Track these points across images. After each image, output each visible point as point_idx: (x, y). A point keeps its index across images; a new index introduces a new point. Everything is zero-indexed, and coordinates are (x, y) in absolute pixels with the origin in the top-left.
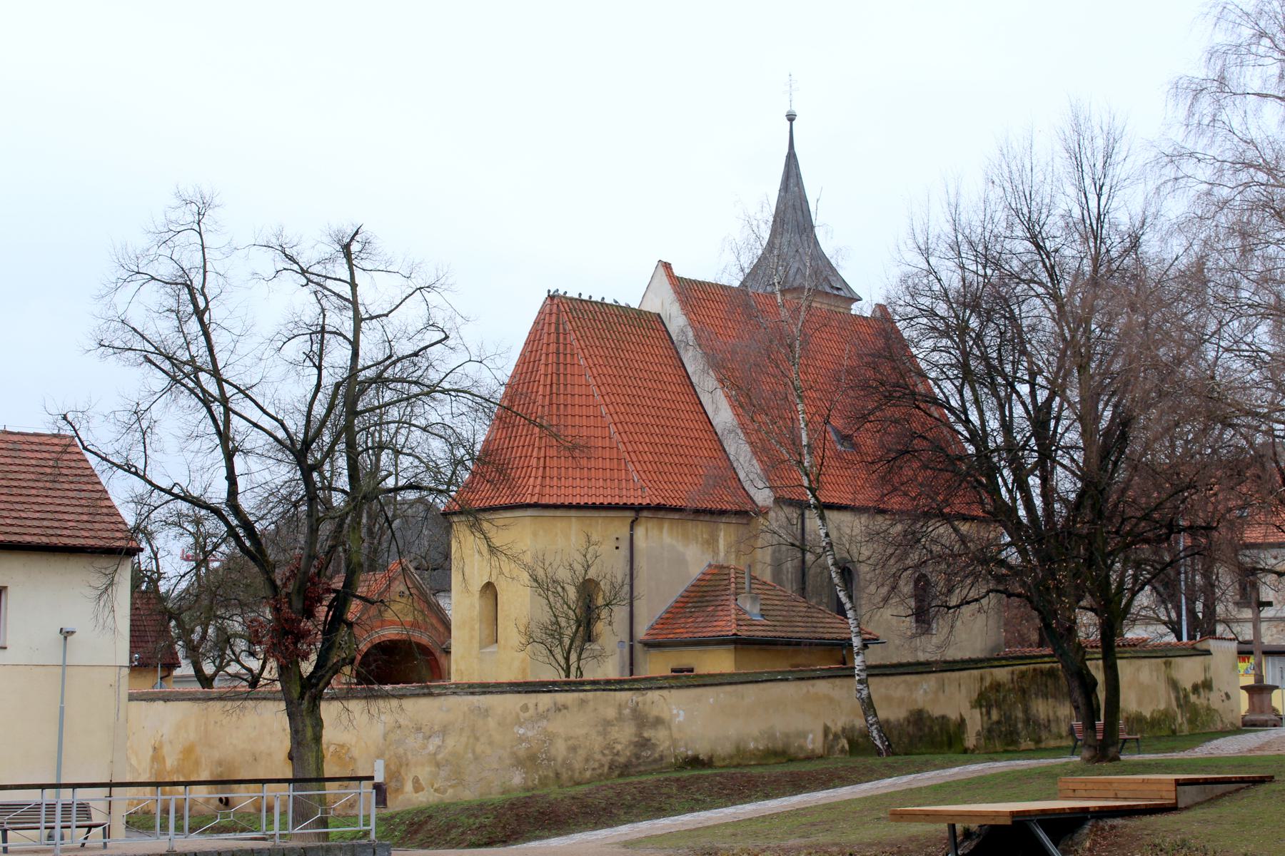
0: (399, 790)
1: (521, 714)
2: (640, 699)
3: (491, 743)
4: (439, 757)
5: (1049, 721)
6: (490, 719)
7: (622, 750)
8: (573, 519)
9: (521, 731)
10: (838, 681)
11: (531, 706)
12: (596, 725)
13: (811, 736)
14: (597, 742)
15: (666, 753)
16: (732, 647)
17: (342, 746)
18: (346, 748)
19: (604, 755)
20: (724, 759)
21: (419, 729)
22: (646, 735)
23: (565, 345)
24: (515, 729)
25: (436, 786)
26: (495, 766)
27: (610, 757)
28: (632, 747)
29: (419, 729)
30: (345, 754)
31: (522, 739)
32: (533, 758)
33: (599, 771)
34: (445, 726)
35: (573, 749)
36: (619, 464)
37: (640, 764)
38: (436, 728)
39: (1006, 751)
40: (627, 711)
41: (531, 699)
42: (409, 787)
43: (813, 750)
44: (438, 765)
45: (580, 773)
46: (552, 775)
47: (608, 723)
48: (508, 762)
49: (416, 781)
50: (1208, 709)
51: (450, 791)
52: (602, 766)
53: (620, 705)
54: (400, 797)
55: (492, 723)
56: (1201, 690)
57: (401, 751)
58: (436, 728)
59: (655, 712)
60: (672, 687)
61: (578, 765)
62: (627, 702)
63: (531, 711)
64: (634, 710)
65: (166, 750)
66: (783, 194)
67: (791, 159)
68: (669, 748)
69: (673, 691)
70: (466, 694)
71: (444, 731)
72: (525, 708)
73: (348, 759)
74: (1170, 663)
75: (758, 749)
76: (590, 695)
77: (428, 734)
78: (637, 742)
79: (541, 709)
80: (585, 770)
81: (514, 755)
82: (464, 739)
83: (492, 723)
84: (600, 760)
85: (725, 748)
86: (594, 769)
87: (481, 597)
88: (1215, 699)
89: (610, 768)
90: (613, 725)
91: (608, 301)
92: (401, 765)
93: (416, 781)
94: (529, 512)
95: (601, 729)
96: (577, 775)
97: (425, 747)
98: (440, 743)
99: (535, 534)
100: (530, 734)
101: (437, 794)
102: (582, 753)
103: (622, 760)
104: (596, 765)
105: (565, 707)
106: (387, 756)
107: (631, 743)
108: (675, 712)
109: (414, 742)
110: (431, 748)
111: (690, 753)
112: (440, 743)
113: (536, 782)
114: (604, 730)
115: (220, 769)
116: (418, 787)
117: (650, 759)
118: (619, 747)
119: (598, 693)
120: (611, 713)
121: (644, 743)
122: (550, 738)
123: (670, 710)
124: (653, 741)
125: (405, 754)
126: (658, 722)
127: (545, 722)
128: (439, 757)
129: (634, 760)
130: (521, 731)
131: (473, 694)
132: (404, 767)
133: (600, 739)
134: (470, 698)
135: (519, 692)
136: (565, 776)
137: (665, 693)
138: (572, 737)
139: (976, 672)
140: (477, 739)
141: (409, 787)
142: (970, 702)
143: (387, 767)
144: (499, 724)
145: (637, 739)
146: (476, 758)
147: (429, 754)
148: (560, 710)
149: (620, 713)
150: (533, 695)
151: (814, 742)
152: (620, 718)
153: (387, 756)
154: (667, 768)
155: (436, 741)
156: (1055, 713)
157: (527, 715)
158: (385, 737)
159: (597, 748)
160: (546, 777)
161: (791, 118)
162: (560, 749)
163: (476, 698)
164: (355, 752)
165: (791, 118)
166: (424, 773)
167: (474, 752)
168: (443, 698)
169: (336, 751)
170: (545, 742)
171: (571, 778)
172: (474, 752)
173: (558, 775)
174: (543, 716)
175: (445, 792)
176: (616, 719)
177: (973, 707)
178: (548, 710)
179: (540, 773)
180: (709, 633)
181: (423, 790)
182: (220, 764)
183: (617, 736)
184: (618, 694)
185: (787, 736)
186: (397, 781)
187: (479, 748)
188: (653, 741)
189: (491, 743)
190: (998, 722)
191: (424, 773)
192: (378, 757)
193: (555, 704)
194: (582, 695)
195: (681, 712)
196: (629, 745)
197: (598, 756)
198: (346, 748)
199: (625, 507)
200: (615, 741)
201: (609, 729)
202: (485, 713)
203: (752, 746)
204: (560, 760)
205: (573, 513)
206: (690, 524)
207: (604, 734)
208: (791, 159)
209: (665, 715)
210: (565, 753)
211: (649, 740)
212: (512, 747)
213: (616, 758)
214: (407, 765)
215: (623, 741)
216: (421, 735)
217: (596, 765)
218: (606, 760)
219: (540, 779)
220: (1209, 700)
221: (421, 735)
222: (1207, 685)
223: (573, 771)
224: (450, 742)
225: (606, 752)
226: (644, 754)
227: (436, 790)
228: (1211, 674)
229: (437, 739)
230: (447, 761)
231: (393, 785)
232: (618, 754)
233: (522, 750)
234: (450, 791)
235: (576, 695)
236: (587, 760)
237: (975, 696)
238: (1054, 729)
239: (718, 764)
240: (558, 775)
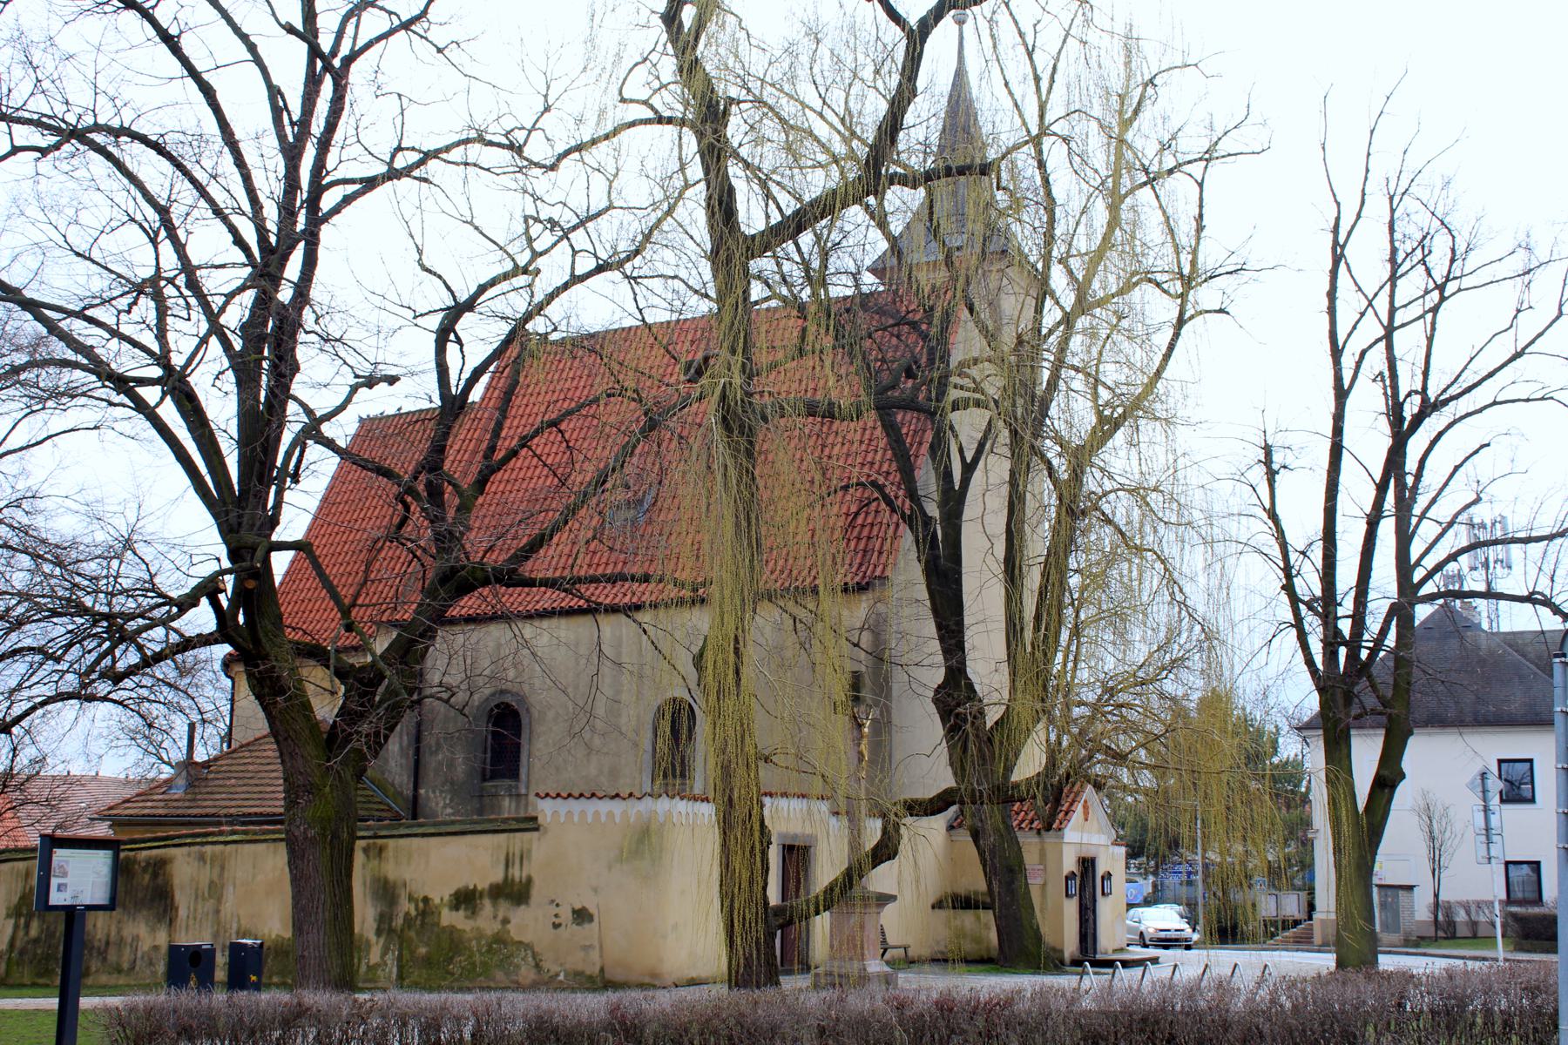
5: (108, 943)
39: (34, 985)
50: (500, 940)
56: (487, 903)
74: (381, 850)
88: (527, 923)
139: (21, 865)
142: (8, 908)
156: (119, 931)
177: (8, 916)
190: (36, 941)
220: (506, 921)
222: (514, 892)
228: (533, 869)
237: (15, 899)
238: (112, 956)
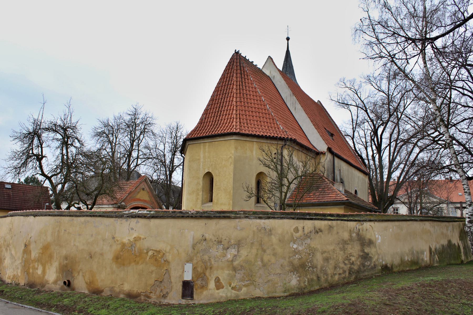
0: (203, 287)
1: (294, 234)
2: (360, 227)
3: (275, 255)
4: (236, 263)
6: (273, 237)
7: (355, 261)
8: (255, 143)
9: (295, 246)
10: (436, 223)
11: (300, 229)
12: (339, 244)
13: (425, 253)
14: (341, 256)
15: (377, 263)
16: (343, 207)
17: (159, 252)
18: (162, 254)
19: (345, 264)
20: (397, 267)
21: (220, 242)
22: (366, 251)
23: (244, 72)
24: (291, 245)
25: (233, 285)
26: (278, 271)
27: (349, 266)
28: (360, 259)
29: (220, 242)
30: (161, 257)
31: (296, 252)
32: (303, 266)
33: (343, 275)
34: (239, 241)
35: (327, 260)
36: (273, 121)
37: (365, 271)
38: (232, 242)
40: (354, 235)
41: (300, 224)
42: (212, 285)
43: (426, 261)
44: (235, 269)
45: (332, 276)
46: (315, 278)
47: (345, 242)
48: (287, 268)
49: (218, 281)
51: (244, 289)
52: (344, 272)
53: (350, 230)
54: (205, 293)
55: (274, 239)
57: (206, 257)
58: (232, 242)
59: (368, 236)
60: (376, 221)
61: (330, 271)
62: (354, 229)
63: (300, 233)
64: (358, 234)
65: (32, 247)
66: (285, 62)
67: (288, 53)
68: (377, 260)
69: (377, 223)
70: (256, 218)
71: (239, 244)
72: (296, 230)
73: (163, 262)
75: (409, 261)
76: (334, 222)
77: (226, 246)
78: (362, 255)
79: (306, 231)
80: (335, 274)
81: (291, 263)
82: (254, 251)
83: (274, 239)
84: (343, 268)
85: (397, 261)
86: (340, 274)
87: (203, 180)
89: (349, 273)
90: (348, 244)
91: (254, 64)
92: (206, 269)
93: (218, 281)
94: (234, 137)
95: (341, 246)
96: (330, 278)
97: (225, 256)
98: (236, 253)
99: (236, 148)
100: (300, 248)
101: (233, 291)
102: (332, 262)
103: (356, 267)
104: (341, 271)
105: (321, 231)
106: (195, 261)
107: (359, 256)
108: (377, 236)
109: (216, 251)
110: (229, 256)
111: (384, 263)
112: (236, 253)
113: (306, 283)
114: (344, 247)
115: (65, 262)
116: (219, 285)
117: (370, 267)
118: (353, 259)
119: (339, 222)
120: (346, 236)
121: (366, 257)
122: (313, 251)
123: (375, 235)
124: (370, 255)
125: (209, 260)
126: (371, 243)
127: (308, 241)
128: (236, 263)
129: (362, 268)
130: (295, 246)
131: (260, 218)
132: (208, 271)
133: (342, 253)
134: (258, 221)
135: (293, 219)
136: (323, 279)
137: (372, 223)
138: (325, 252)
140: (264, 251)
141: (212, 285)
143: (194, 269)
144: (280, 241)
145: (362, 254)
146: (264, 265)
147: (228, 261)
148: (318, 232)
149: (351, 236)
150: (301, 221)
151: (426, 257)
152: (351, 239)
153: (195, 261)
154: (378, 273)
155: (233, 251)
157: (298, 235)
158: (194, 247)
159: (341, 259)
160: (312, 280)
161: (288, 39)
162: (319, 259)
163: (263, 221)
164: (169, 257)
165: (288, 39)
166: (224, 275)
167: (262, 260)
168: (237, 220)
169: (153, 255)
170: (310, 254)
171: (326, 280)
172: (262, 260)
173: (318, 278)
174: (307, 236)
175: (240, 289)
176: (349, 240)
178: (311, 232)
179: (308, 276)
180: (326, 199)
181: (223, 287)
182: (66, 258)
183: (351, 251)
184: (349, 223)
185: (417, 252)
186: (202, 280)
187: (266, 258)
188: (370, 255)
189: (275, 255)
191: (224, 275)
192: (188, 262)
193: (315, 228)
194: (330, 222)
195: (380, 236)
196: (358, 258)
197: (342, 265)
198: (162, 254)
199: (281, 139)
200: (351, 255)
201: (346, 246)
202: (270, 232)
203: (406, 259)
204: (319, 267)
205: (255, 140)
206: (300, 153)
207: (344, 249)
208: (288, 53)
209: (373, 238)
210: (322, 263)
211: (368, 254)
212: (290, 257)
213: (352, 266)
214: (211, 268)
215: (355, 254)
216: (221, 246)
217: (341, 271)
218: (346, 268)
219: (308, 282)
221: (221, 246)
223: (327, 275)
224: (244, 252)
225: (346, 262)
226: (366, 263)
227: (233, 288)
229: (233, 250)
230: (241, 266)
231: (199, 282)
232: (353, 264)
233: (296, 260)
234: (244, 289)
235: (326, 222)
236: (335, 268)
239: (395, 270)
240: (318, 278)
